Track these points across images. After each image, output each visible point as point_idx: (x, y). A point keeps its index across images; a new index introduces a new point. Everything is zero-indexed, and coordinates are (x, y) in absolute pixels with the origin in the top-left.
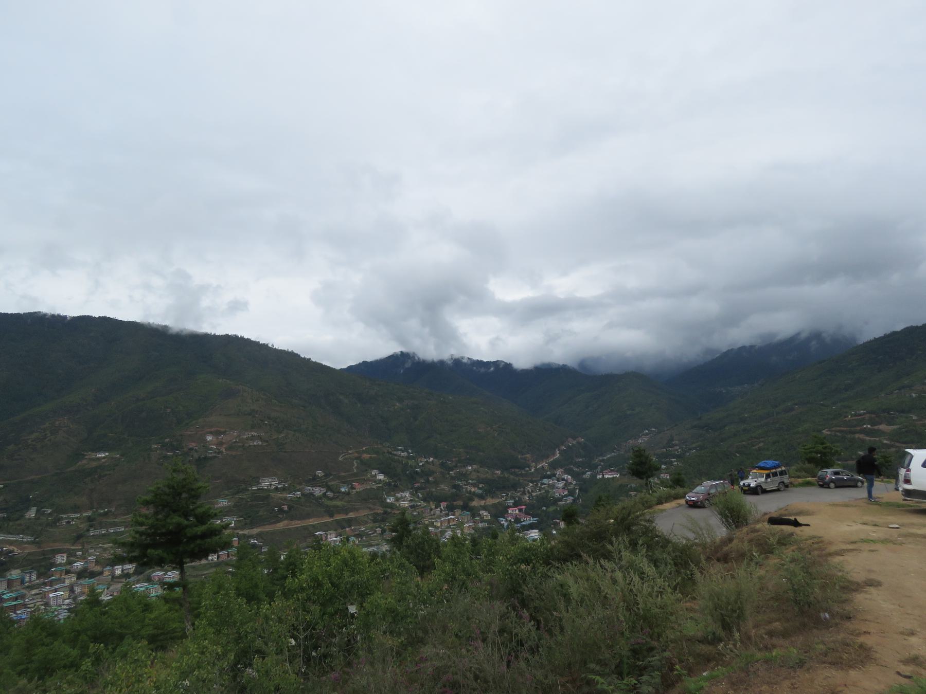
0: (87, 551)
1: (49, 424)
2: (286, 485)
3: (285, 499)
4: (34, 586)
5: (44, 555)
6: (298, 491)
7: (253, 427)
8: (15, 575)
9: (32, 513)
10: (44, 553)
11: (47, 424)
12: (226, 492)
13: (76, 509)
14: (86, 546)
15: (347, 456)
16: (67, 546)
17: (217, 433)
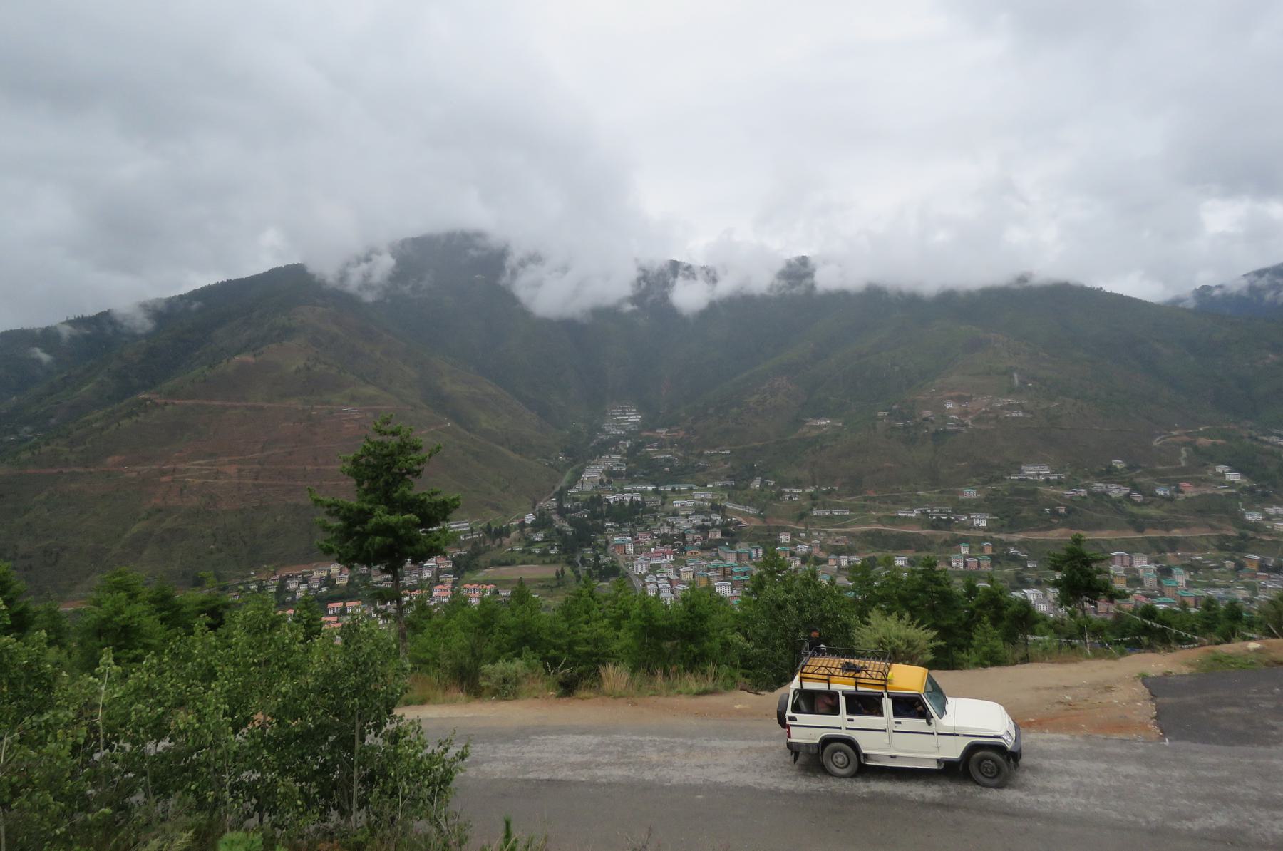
0: (811, 534)
2: (1063, 477)
3: (1062, 497)
6: (1083, 487)
7: (1011, 391)
9: (756, 484)
10: (769, 529)
12: (975, 480)
13: (798, 483)
14: (810, 528)
15: (1168, 440)
16: (791, 525)
17: (959, 399)
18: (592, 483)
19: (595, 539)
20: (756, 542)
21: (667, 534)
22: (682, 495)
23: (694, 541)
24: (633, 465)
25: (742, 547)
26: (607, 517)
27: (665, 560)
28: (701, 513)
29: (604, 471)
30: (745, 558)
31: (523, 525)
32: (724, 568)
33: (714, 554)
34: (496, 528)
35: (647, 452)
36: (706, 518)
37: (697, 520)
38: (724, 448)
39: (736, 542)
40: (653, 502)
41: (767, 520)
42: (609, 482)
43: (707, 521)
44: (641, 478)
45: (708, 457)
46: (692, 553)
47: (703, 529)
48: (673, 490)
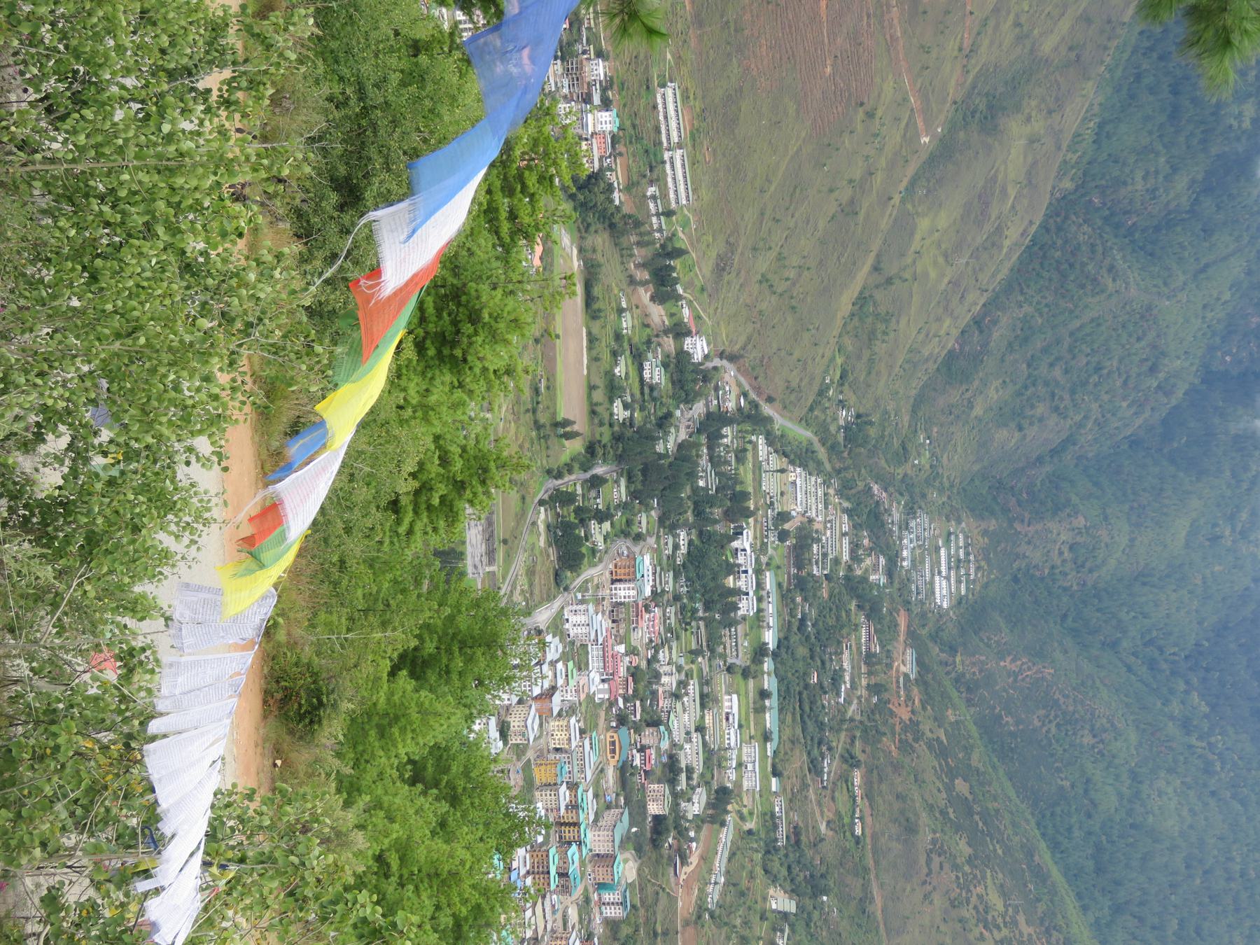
5: (665, 933)
9: (780, 901)
18: (782, 494)
19: (648, 508)
21: (658, 683)
22: (752, 716)
23: (642, 749)
24: (825, 595)
25: (627, 869)
26: (701, 534)
27: (597, 679)
28: (708, 762)
29: (811, 521)
31: (679, 331)
32: (576, 824)
33: (611, 797)
34: (673, 269)
35: (857, 627)
36: (695, 776)
37: (691, 755)
38: (869, 820)
39: (639, 850)
40: (737, 648)
41: (690, 930)
42: (783, 536)
43: (689, 778)
44: (792, 615)
45: (847, 780)
46: (613, 743)
47: (671, 769)
48: (764, 694)
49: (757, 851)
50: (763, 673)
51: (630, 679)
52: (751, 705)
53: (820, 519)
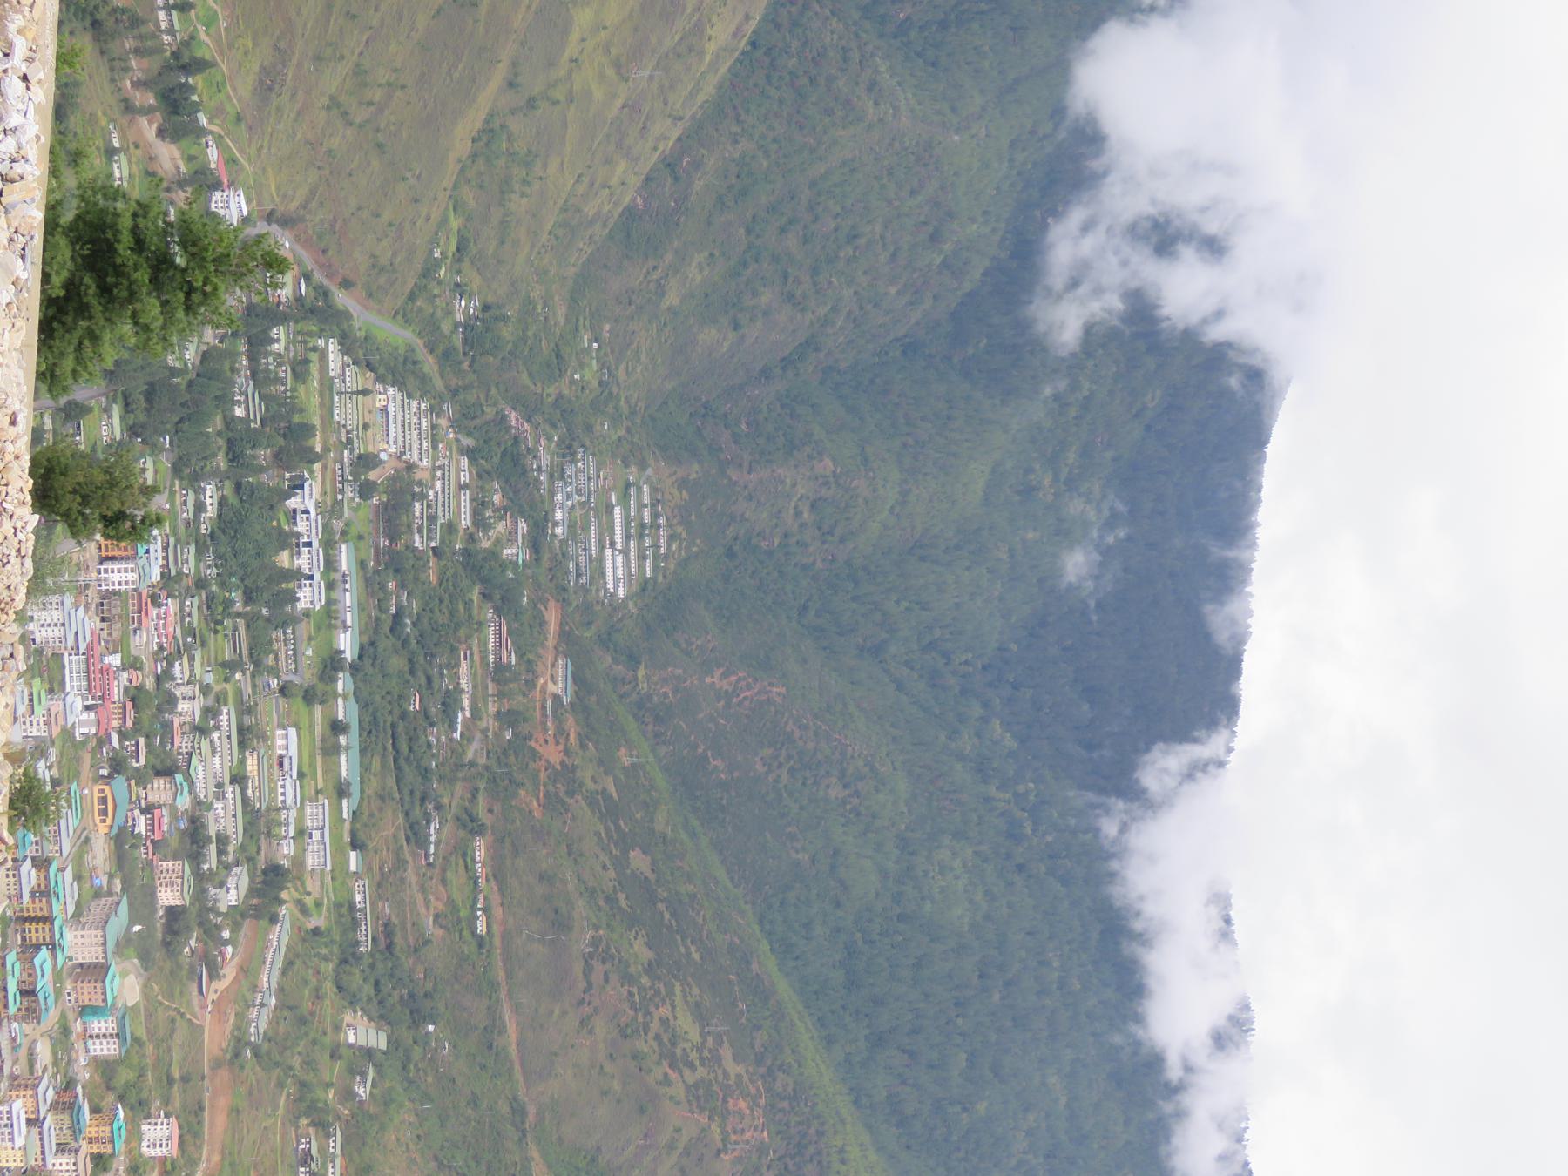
1: (739, 1076)
4: (69, 1049)
5: (185, 1079)
8: (122, 985)
9: (361, 1032)
11: (740, 1069)
18: (366, 426)
19: (155, 449)
20: (142, 1033)
22: (319, 759)
23: (148, 810)
24: (433, 578)
25: (126, 986)
26: (238, 487)
27: (79, 704)
29: (410, 467)
30: (87, 993)
31: (204, 182)
32: (48, 920)
33: (102, 881)
34: (192, 89)
36: (231, 849)
37: (224, 818)
38: (498, 912)
39: (145, 958)
41: (224, 1074)
42: (366, 490)
43: (221, 852)
44: (381, 608)
45: (465, 854)
46: (103, 800)
47: (194, 837)
48: (337, 727)
49: (326, 959)
50: (336, 695)
51: (129, 705)
52: (318, 744)
53: (425, 463)
